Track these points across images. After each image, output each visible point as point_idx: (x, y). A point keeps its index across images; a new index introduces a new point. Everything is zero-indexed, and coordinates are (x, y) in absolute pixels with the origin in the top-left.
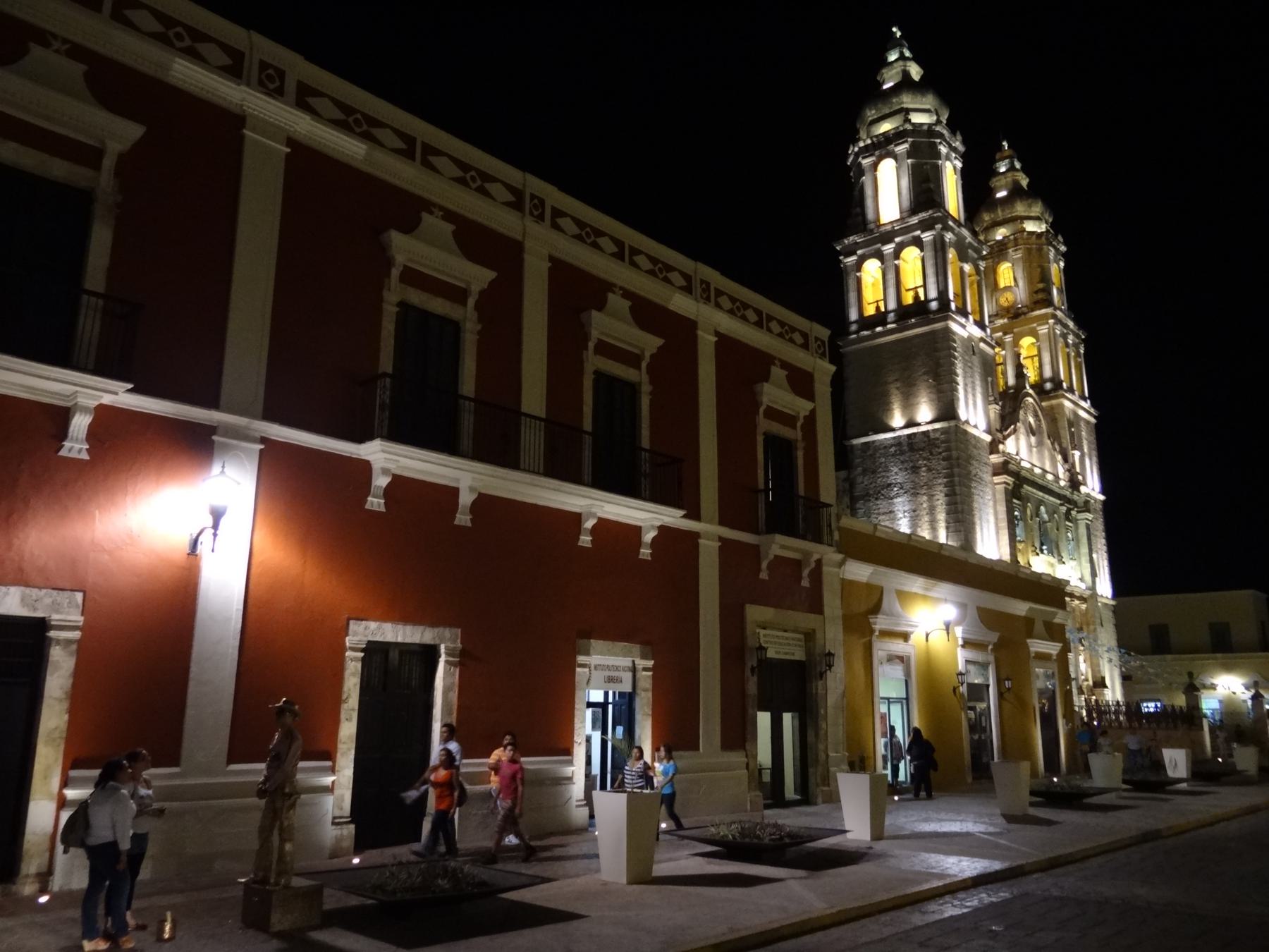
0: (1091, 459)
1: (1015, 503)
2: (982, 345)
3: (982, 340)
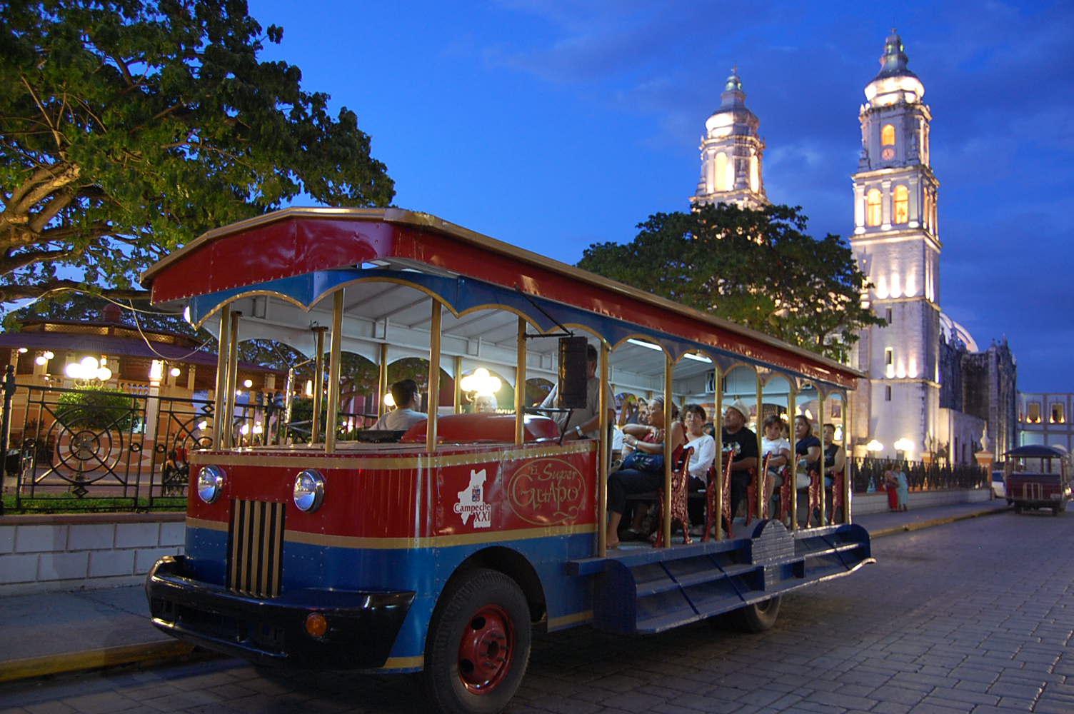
0: (903, 272)
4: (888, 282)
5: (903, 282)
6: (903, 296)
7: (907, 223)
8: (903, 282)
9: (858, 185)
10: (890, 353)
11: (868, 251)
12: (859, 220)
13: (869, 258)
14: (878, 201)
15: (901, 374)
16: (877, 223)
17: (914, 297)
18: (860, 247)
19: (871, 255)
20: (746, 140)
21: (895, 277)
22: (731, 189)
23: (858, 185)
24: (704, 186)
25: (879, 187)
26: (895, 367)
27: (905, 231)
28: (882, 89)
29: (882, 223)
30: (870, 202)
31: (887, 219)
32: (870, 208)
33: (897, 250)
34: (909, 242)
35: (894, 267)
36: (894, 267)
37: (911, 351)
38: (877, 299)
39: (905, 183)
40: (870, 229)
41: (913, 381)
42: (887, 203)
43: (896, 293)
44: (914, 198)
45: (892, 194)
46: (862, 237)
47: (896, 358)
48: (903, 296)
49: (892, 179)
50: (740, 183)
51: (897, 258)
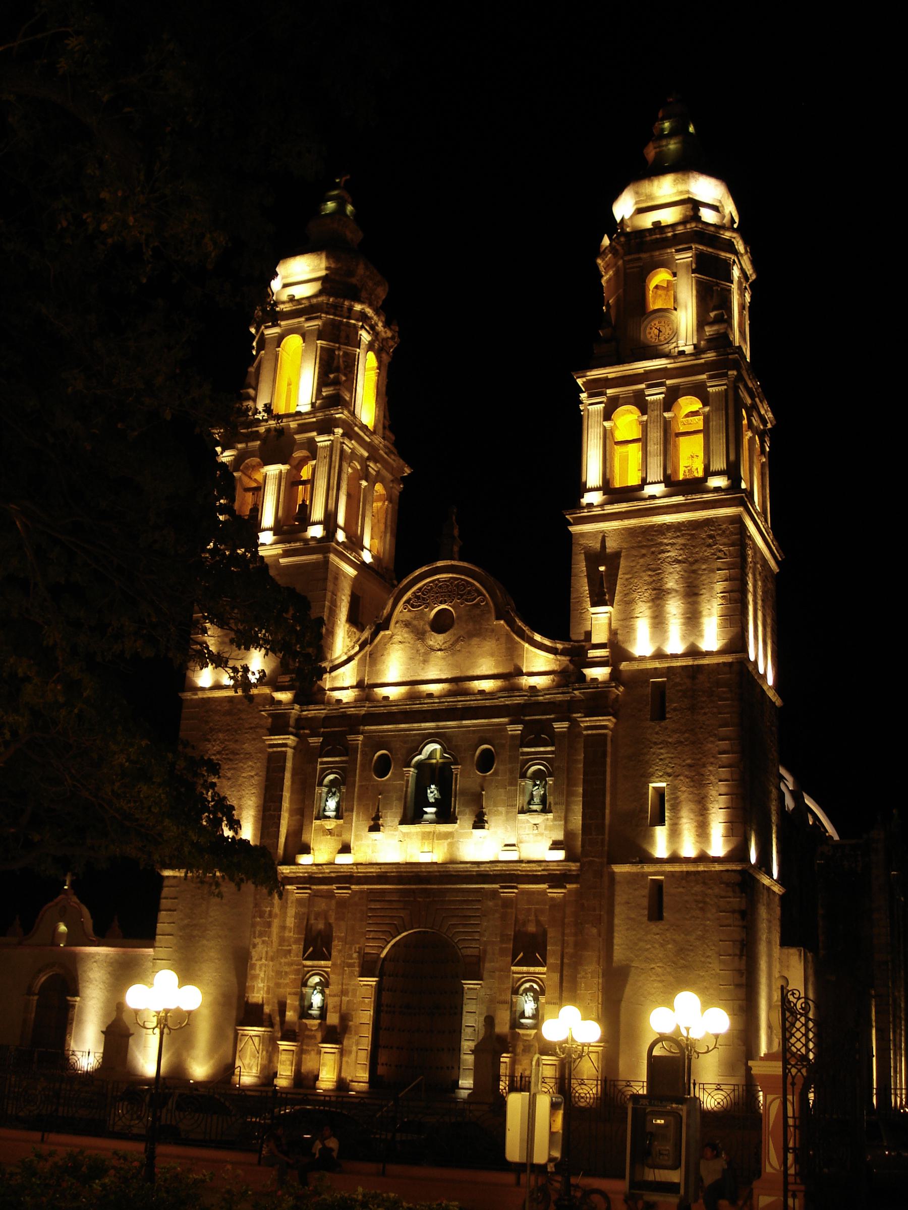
1: (322, 763)
2: (281, 560)
3: (286, 554)
4: (659, 622)
5: (692, 619)
6: (693, 652)
7: (704, 479)
8: (692, 619)
9: (591, 396)
10: (660, 793)
11: (612, 545)
12: (593, 474)
13: (613, 560)
14: (636, 433)
15: (689, 849)
16: (633, 480)
17: (720, 652)
18: (594, 534)
19: (617, 555)
20: (350, 309)
21: (674, 608)
22: (306, 408)
23: (591, 396)
24: (250, 404)
25: (642, 405)
26: (675, 834)
27: (698, 498)
28: (650, 197)
29: (644, 482)
30: (620, 436)
31: (655, 473)
32: (619, 449)
33: (681, 541)
34: (708, 522)
35: (672, 582)
36: (672, 582)
37: (713, 792)
38: (630, 658)
39: (699, 391)
40: (613, 493)
41: (718, 867)
42: (655, 435)
43: (675, 644)
44: (718, 423)
45: (666, 415)
46: (597, 511)
47: (675, 808)
48: (693, 652)
49: (668, 382)
50: (327, 397)
51: (679, 562)
